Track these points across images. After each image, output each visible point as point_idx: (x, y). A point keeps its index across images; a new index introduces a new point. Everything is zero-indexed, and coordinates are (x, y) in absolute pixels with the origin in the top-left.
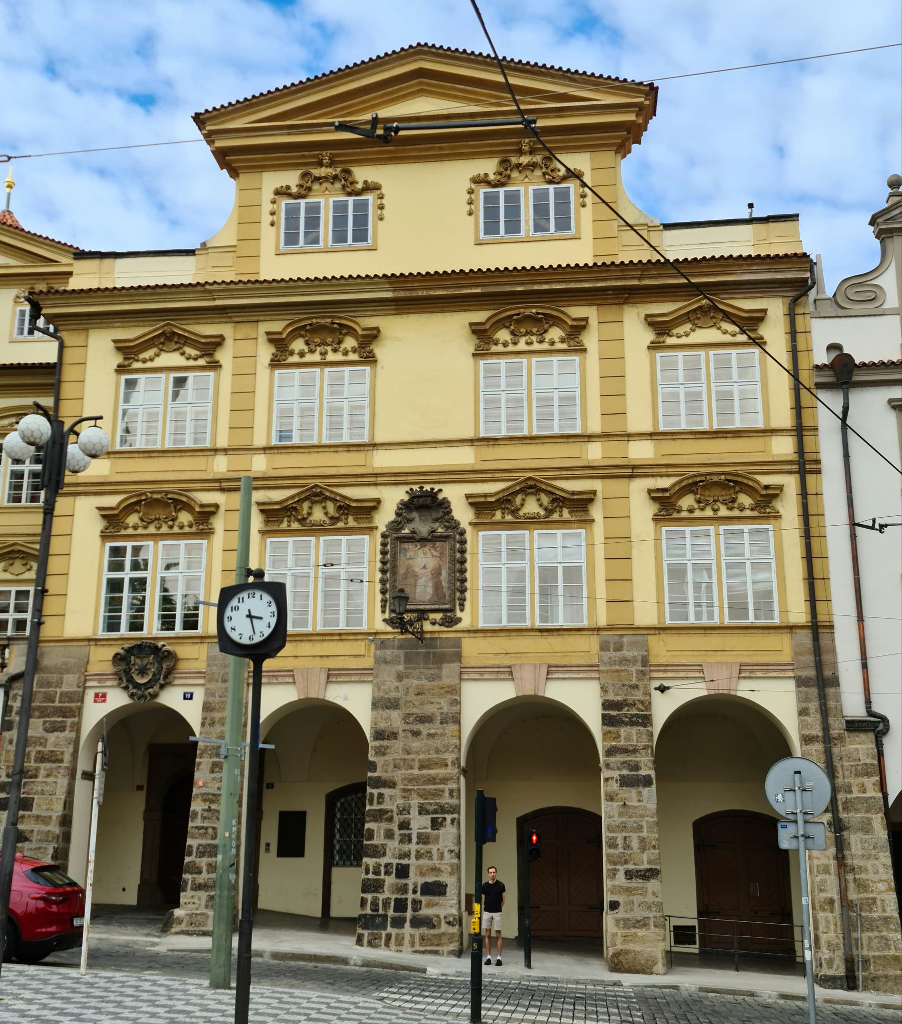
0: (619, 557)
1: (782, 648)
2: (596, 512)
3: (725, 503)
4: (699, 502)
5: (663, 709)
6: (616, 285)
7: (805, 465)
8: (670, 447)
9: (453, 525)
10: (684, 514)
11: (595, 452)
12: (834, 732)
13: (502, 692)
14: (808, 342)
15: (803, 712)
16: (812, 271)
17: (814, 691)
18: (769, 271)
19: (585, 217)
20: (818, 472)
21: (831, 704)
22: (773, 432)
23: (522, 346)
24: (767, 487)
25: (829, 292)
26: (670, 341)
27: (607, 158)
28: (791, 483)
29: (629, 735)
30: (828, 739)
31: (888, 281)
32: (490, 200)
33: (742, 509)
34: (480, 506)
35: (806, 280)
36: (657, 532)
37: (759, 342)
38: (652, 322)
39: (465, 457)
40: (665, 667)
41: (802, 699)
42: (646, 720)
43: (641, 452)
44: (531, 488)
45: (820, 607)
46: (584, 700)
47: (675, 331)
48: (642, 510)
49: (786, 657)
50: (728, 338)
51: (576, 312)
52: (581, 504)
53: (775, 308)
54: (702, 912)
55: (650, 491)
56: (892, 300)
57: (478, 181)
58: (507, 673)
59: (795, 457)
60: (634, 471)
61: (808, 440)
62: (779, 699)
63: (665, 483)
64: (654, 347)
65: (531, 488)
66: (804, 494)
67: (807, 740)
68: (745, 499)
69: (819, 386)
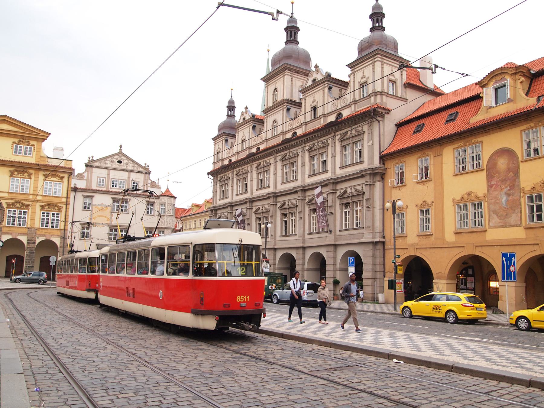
0: (33, 216)
2: (30, 208)
5: (38, 241)
6: (39, 168)
7: (67, 204)
8: (44, 198)
9: (3, 207)
11: (31, 197)
13: (10, 237)
19: (34, 154)
23: (19, 176)
27: (40, 143)
28: (64, 206)
29: (31, 245)
30: (64, 247)
31: (85, 175)
32: (16, 147)
34: (8, 205)
37: (63, 182)
38: (44, 175)
39: (6, 195)
40: (39, 235)
41: (61, 241)
42: (35, 243)
43: (39, 198)
44: (18, 202)
46: (24, 239)
48: (38, 208)
49: (59, 234)
51: (31, 171)
52: (27, 206)
53: (66, 176)
56: (85, 178)
57: (14, 143)
58: (11, 234)
60: (38, 201)
62: (57, 241)
63: (43, 204)
65: (18, 202)
66: (66, 208)
67: (60, 247)
68: (56, 208)
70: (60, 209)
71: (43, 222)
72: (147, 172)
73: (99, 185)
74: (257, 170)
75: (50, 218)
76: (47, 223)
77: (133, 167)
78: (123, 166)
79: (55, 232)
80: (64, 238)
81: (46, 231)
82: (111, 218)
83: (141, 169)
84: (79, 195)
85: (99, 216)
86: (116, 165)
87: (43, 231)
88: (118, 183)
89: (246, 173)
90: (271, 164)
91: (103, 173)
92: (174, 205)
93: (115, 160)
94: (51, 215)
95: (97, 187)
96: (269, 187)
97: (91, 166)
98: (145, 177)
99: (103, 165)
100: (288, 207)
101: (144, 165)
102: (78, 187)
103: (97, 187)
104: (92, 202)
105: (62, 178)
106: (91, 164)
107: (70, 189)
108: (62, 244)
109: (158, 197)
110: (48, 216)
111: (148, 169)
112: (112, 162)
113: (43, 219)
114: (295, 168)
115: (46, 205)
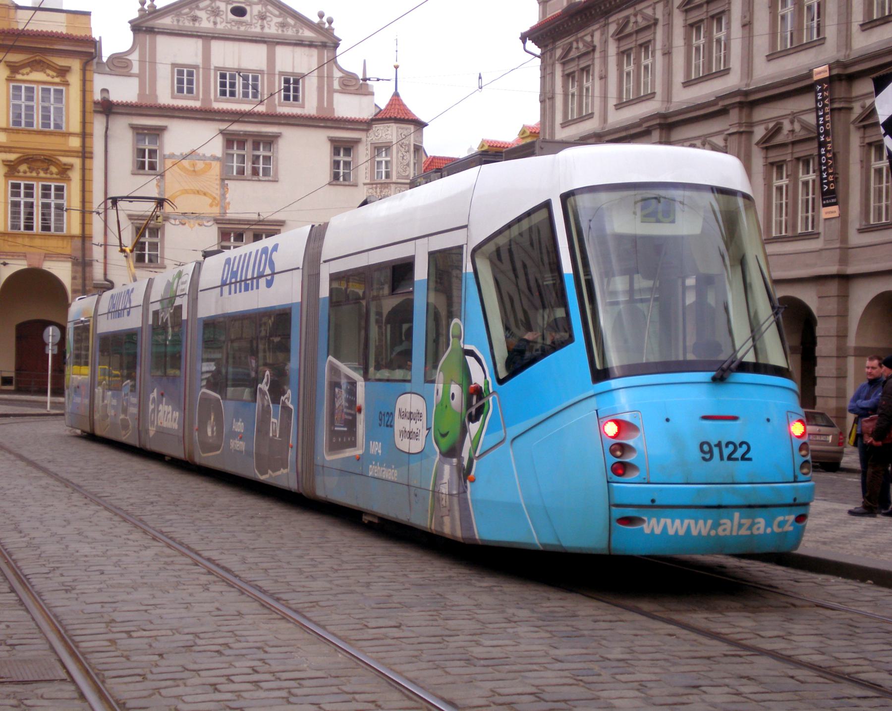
1: (67, 248)
3: (43, 169)
4: (29, 168)
7: (85, 154)
10: (21, 174)
12: (87, 288)
14: (92, 87)
15: (74, 278)
16: (95, 48)
17: (80, 269)
18: (72, 46)
20: (91, 158)
21: (87, 275)
22: (70, 134)
24: (65, 165)
25: (105, 59)
26: (19, 77)
28: (77, 162)
31: (134, 57)
33: (52, 174)
35: (92, 53)
36: (7, 183)
41: (74, 271)
45: (87, 227)
47: (21, 71)
49: (68, 251)
50: (49, 79)
53: (75, 65)
54: (18, 369)
55: (3, 161)
56: (135, 69)
59: (80, 149)
61: (87, 140)
62: (63, 271)
63: (13, 157)
64: (9, 79)
66: (83, 169)
68: (54, 169)
69: (95, 112)
70: (64, 170)
71: (15, 214)
72: (325, 41)
73: (180, 90)
74: (564, 64)
75: (38, 200)
76: (30, 216)
77: (283, 25)
78: (252, 24)
79: (53, 245)
80: (83, 264)
81: (27, 241)
82: (223, 196)
83: (308, 34)
84: (121, 127)
85: (186, 192)
86: (226, 22)
87: (20, 240)
88: (239, 82)
89: (586, 54)
90: (656, 22)
91: (187, 51)
92: (418, 149)
93: (222, 6)
94: (38, 191)
95: (173, 97)
96: (726, 71)
97: (151, 31)
98: (320, 58)
99: (187, 24)
100: (791, 139)
101: (316, 20)
102: (114, 97)
103: (173, 97)
104: (161, 147)
105: (63, 72)
106: (150, 24)
107: (90, 107)
108: (79, 281)
109: (366, 125)
110: (30, 195)
111: (329, 32)
112: (216, 13)
113: (16, 205)
114: (722, 35)
115: (20, 161)
